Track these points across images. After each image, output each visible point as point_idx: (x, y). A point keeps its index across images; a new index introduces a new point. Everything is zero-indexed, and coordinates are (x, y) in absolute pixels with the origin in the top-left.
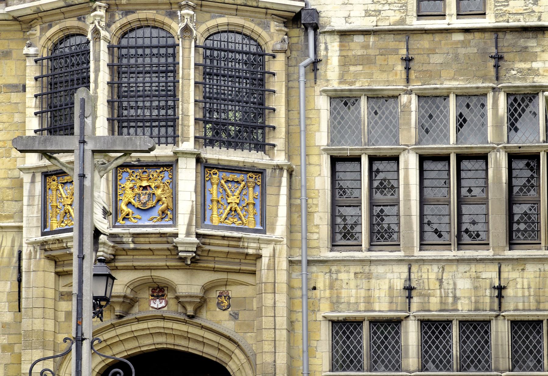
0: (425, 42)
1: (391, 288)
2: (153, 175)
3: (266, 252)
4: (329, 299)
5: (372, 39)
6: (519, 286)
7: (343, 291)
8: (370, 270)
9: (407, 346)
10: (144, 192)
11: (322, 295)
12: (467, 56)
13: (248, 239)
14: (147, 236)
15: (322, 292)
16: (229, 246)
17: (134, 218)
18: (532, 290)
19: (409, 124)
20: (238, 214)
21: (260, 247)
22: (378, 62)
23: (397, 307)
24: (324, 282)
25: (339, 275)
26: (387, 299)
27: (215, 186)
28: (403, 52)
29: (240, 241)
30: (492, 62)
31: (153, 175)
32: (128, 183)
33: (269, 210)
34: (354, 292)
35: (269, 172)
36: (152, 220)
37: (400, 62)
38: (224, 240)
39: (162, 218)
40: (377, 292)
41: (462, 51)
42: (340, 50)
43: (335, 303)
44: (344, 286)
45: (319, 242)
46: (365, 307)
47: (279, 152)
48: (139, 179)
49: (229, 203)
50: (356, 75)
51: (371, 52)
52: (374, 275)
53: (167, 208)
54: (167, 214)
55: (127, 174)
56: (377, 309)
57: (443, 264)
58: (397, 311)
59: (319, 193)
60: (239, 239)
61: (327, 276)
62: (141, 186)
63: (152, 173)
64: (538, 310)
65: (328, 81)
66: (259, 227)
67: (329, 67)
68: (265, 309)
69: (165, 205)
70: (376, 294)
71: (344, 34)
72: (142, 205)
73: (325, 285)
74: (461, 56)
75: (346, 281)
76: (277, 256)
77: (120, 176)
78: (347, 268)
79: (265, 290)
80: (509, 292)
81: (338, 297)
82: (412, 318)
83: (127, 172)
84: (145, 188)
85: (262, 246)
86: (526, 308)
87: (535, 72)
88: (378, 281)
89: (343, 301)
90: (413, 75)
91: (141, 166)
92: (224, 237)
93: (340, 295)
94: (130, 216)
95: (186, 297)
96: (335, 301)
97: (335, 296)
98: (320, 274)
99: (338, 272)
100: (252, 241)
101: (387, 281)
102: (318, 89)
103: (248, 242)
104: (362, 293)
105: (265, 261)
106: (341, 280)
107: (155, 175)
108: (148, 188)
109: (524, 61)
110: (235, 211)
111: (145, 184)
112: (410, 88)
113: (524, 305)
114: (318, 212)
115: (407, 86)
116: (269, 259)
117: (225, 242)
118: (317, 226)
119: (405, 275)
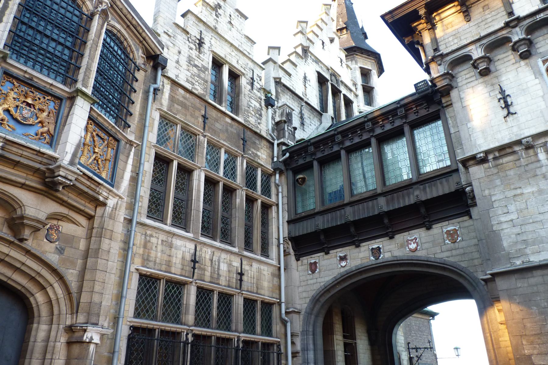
0: (213, 113)
1: (183, 258)
2: (39, 99)
3: (111, 202)
4: (142, 256)
5: (188, 95)
6: (249, 276)
7: (152, 251)
8: (172, 241)
9: (187, 305)
10: (28, 108)
11: (137, 252)
12: (232, 132)
13: (105, 187)
14: (22, 148)
15: (138, 248)
16: (88, 187)
17: (8, 126)
18: (255, 280)
19: (203, 154)
20: (98, 164)
21: (108, 197)
22: (190, 110)
23: (185, 274)
24: (140, 241)
25: (152, 238)
26: (180, 266)
27: (89, 134)
28: (203, 113)
29: (97, 187)
30: (242, 142)
31: (39, 99)
32: (12, 92)
33: (119, 171)
34: (159, 254)
35: (123, 143)
36: (27, 136)
37: (201, 117)
38: (88, 181)
39: (40, 139)
40: (174, 258)
41: (230, 128)
42: (171, 91)
43: (146, 260)
44: (154, 248)
45: (141, 209)
46: (166, 269)
47: (131, 133)
48: (24, 95)
49: (94, 152)
50: (178, 112)
51: (188, 103)
52: (174, 245)
53: (48, 132)
54: (45, 138)
55: (11, 85)
56: (173, 272)
57: (213, 250)
58: (185, 276)
59: (146, 173)
60: (99, 184)
61: (143, 237)
62: (24, 102)
63: (38, 96)
64: (257, 293)
65: (161, 104)
66: (109, 181)
67: (163, 97)
68: (101, 252)
69: (45, 129)
70: (174, 260)
71: (174, 83)
72: (22, 118)
73: (140, 244)
74: (229, 131)
75: (155, 245)
76: (117, 209)
77: (3, 82)
78: (157, 235)
79: (104, 235)
80: (245, 278)
81: (148, 256)
82: (194, 284)
83: (13, 83)
84: (29, 105)
85: (110, 197)
86: (252, 291)
87: (258, 157)
88: (176, 251)
89: (151, 259)
90: (207, 128)
91: (31, 86)
92: (90, 178)
93: (150, 255)
94: (5, 122)
95: (33, 220)
96: (146, 258)
97: (147, 254)
98: (138, 234)
99: (151, 236)
100: (106, 190)
101: (181, 253)
102: (155, 106)
103: (102, 190)
104: (165, 258)
105: (108, 209)
106: (152, 243)
107: (42, 100)
108: (32, 106)
109: (255, 149)
110: (97, 161)
111: (30, 101)
112: (204, 134)
113: (251, 288)
114: (144, 186)
115: (204, 132)
116: (112, 210)
117: (88, 183)
118: (141, 197)
119: (192, 251)
